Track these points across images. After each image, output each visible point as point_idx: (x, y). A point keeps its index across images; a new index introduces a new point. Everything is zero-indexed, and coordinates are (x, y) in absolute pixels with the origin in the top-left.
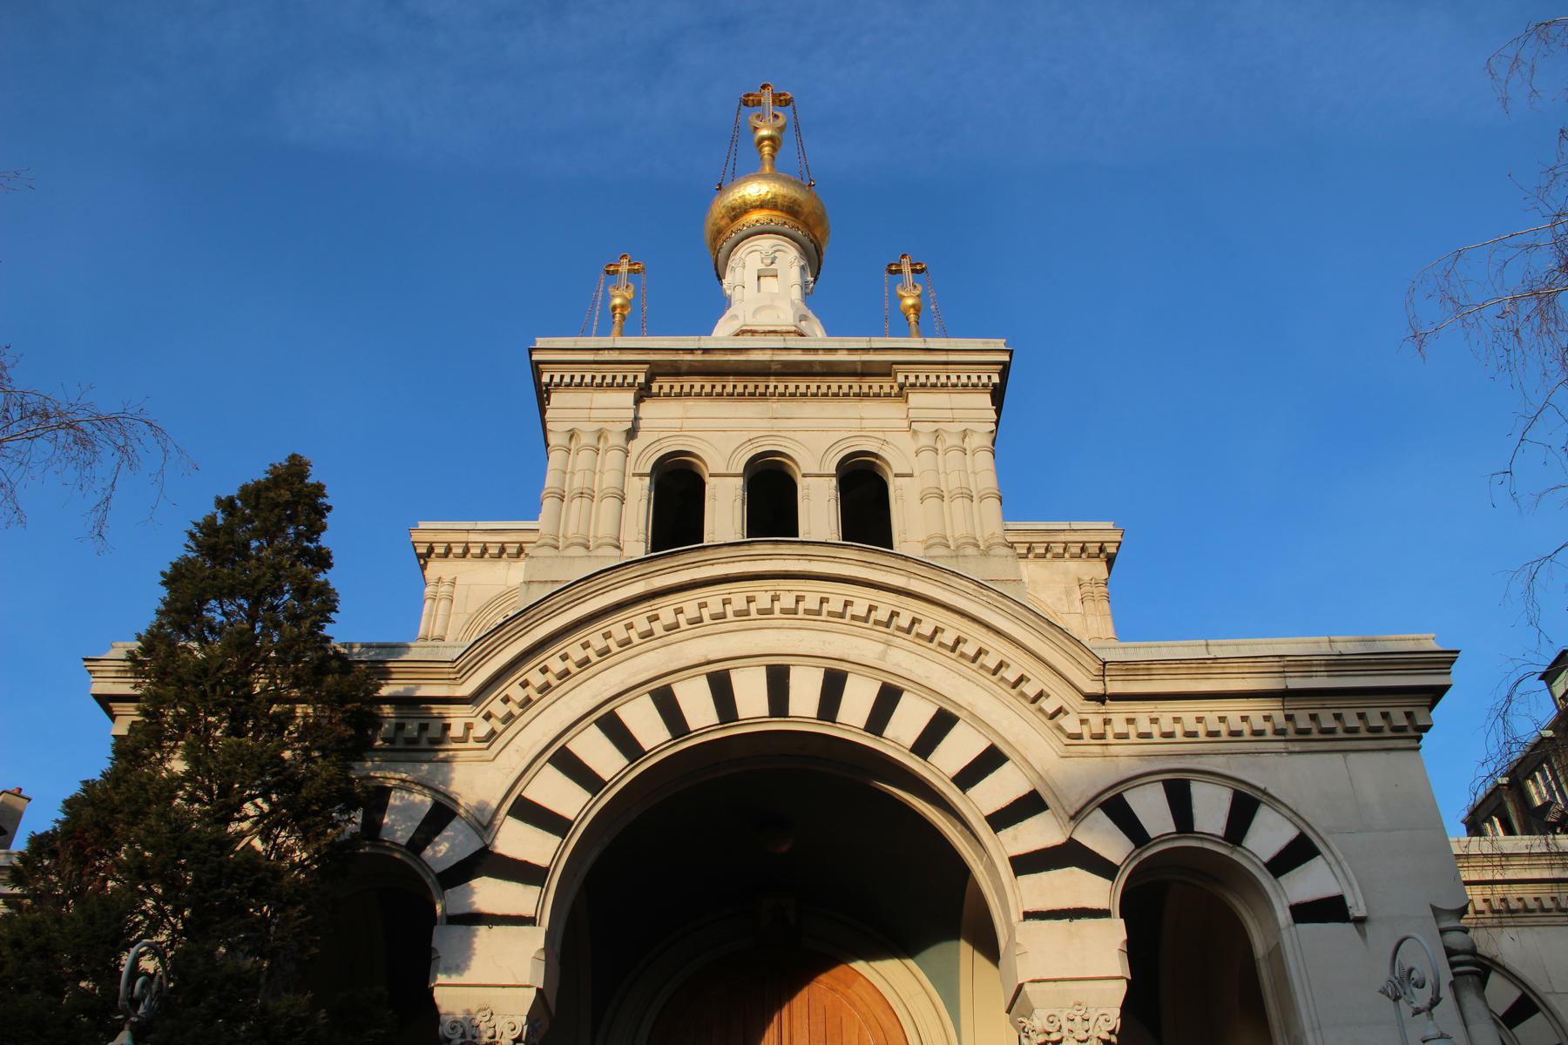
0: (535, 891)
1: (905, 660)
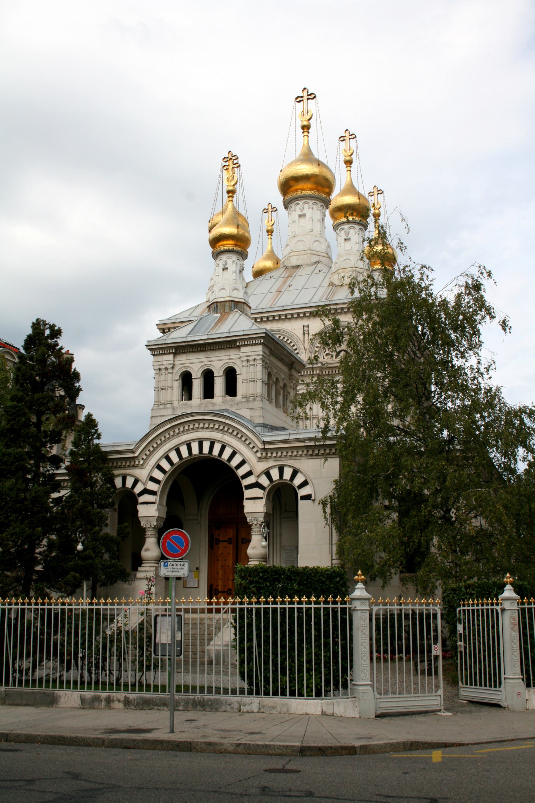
0: (155, 497)
1: (227, 439)
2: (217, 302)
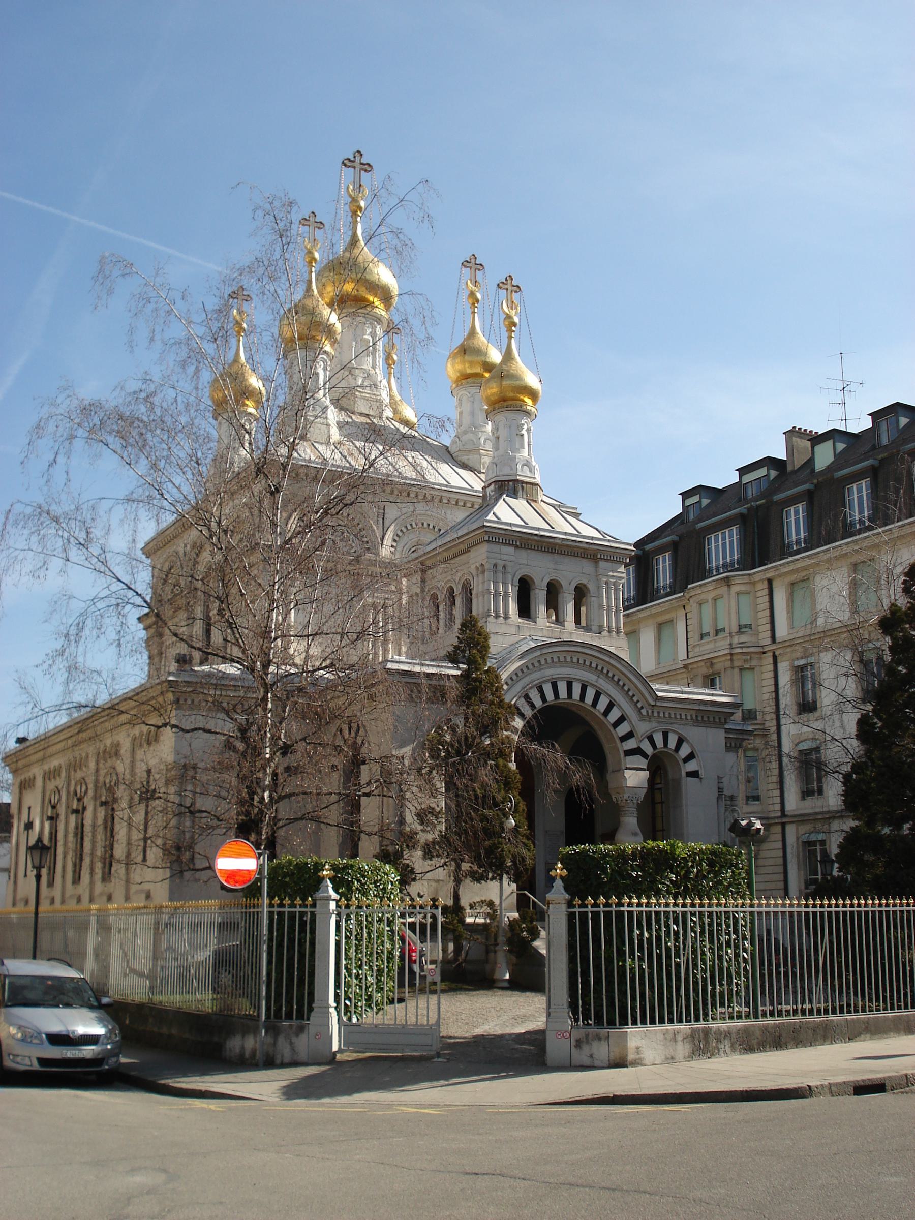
2: (522, 482)
